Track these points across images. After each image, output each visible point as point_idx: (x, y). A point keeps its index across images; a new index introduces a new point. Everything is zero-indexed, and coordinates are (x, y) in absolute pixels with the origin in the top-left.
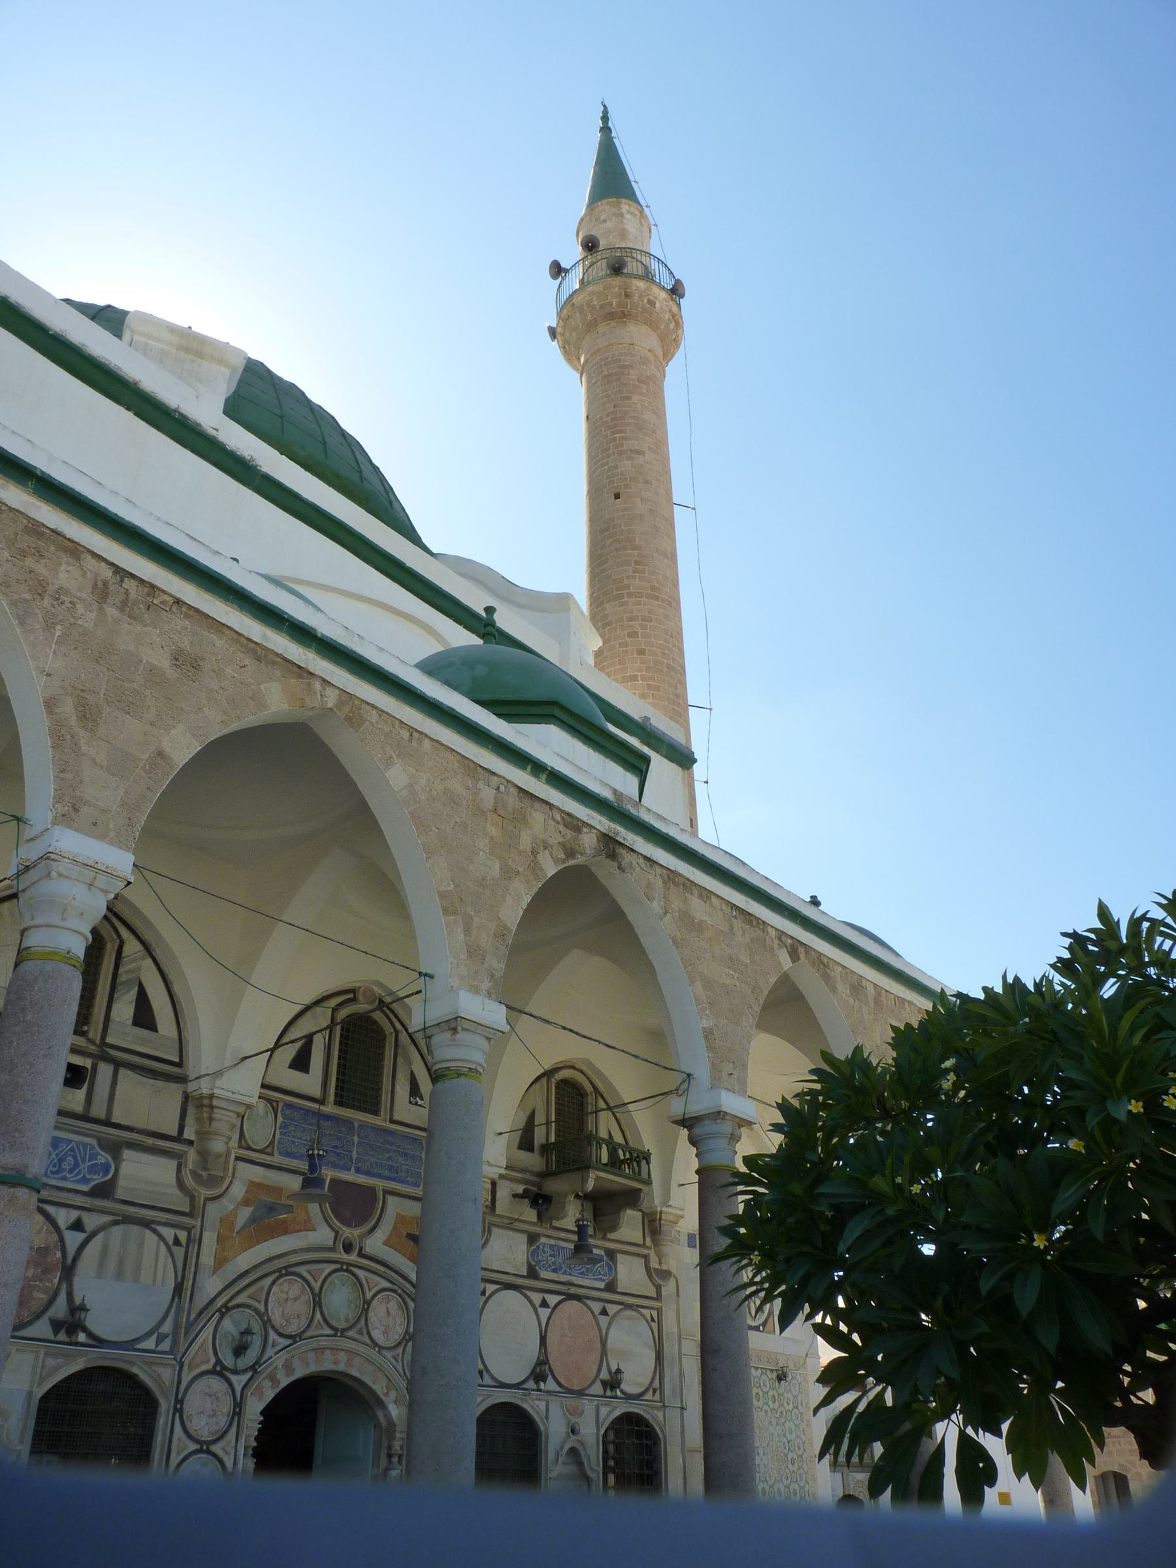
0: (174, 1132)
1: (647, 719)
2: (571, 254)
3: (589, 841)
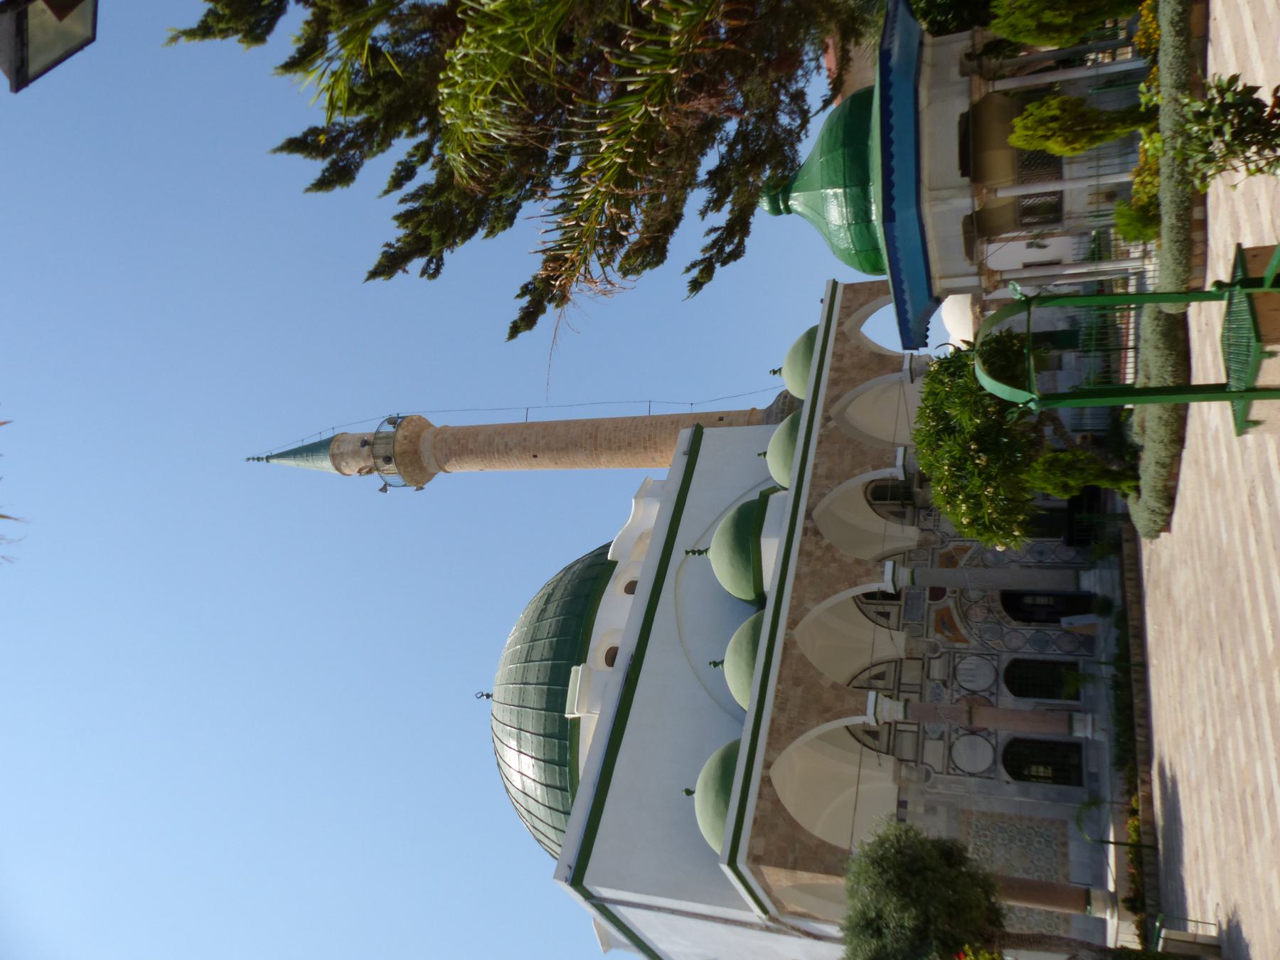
0: (920, 662)
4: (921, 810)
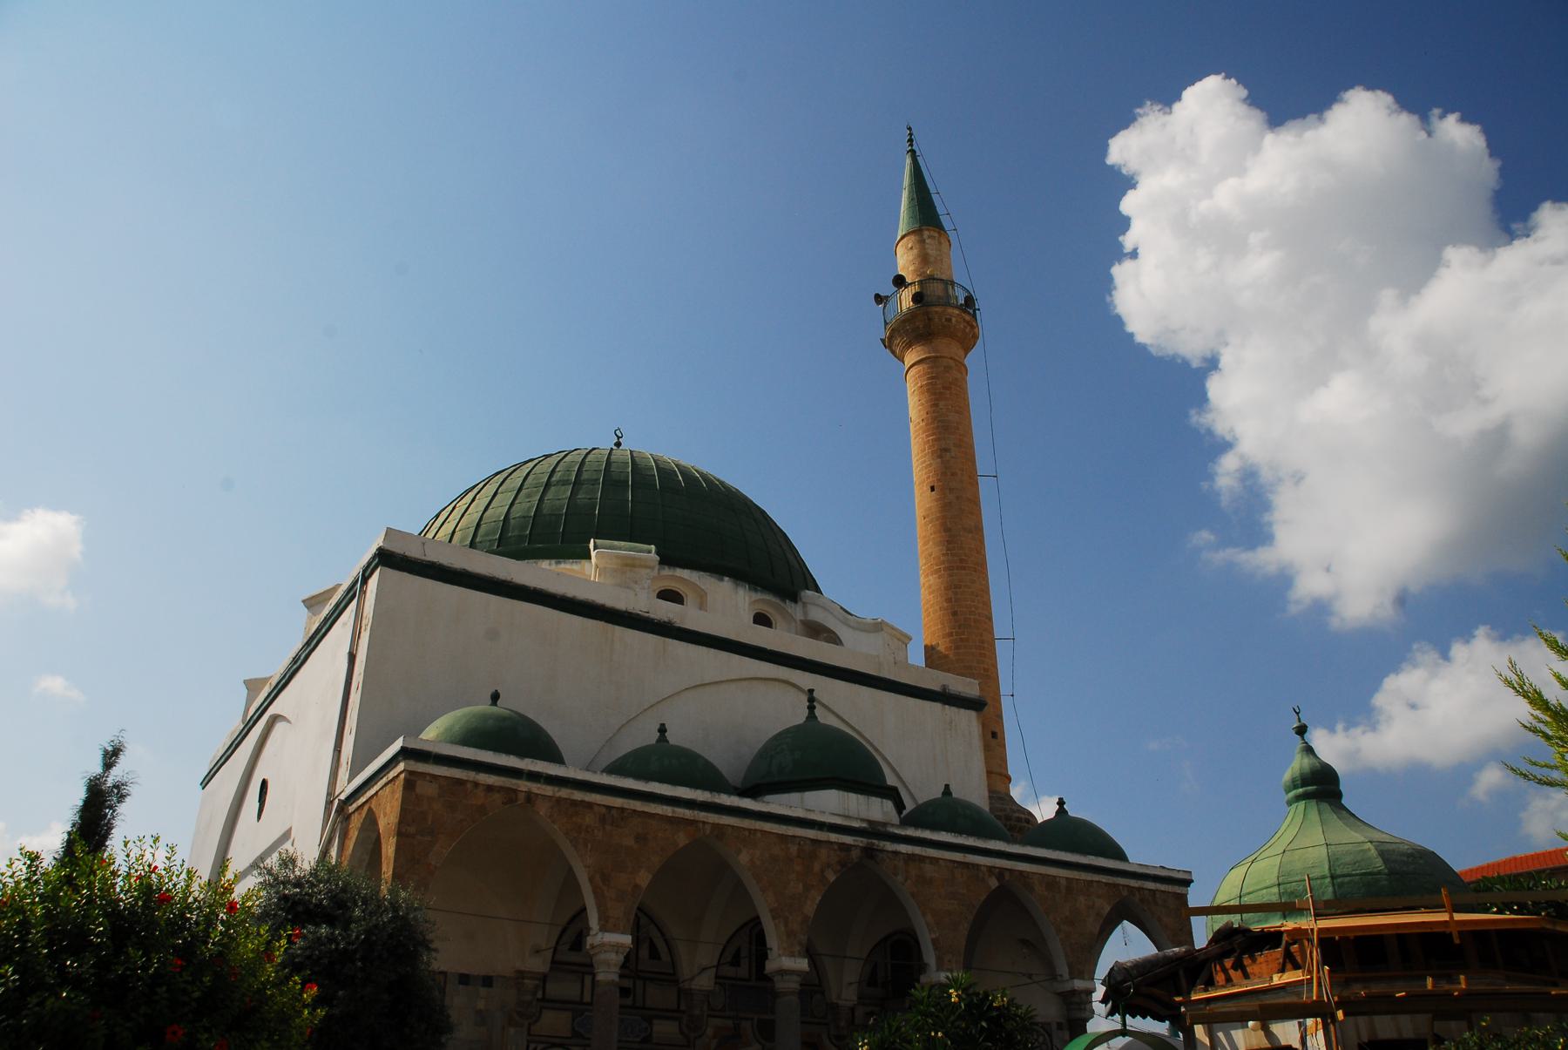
1: (944, 687)
2: (887, 289)
3: (855, 854)
4: (481, 1005)
